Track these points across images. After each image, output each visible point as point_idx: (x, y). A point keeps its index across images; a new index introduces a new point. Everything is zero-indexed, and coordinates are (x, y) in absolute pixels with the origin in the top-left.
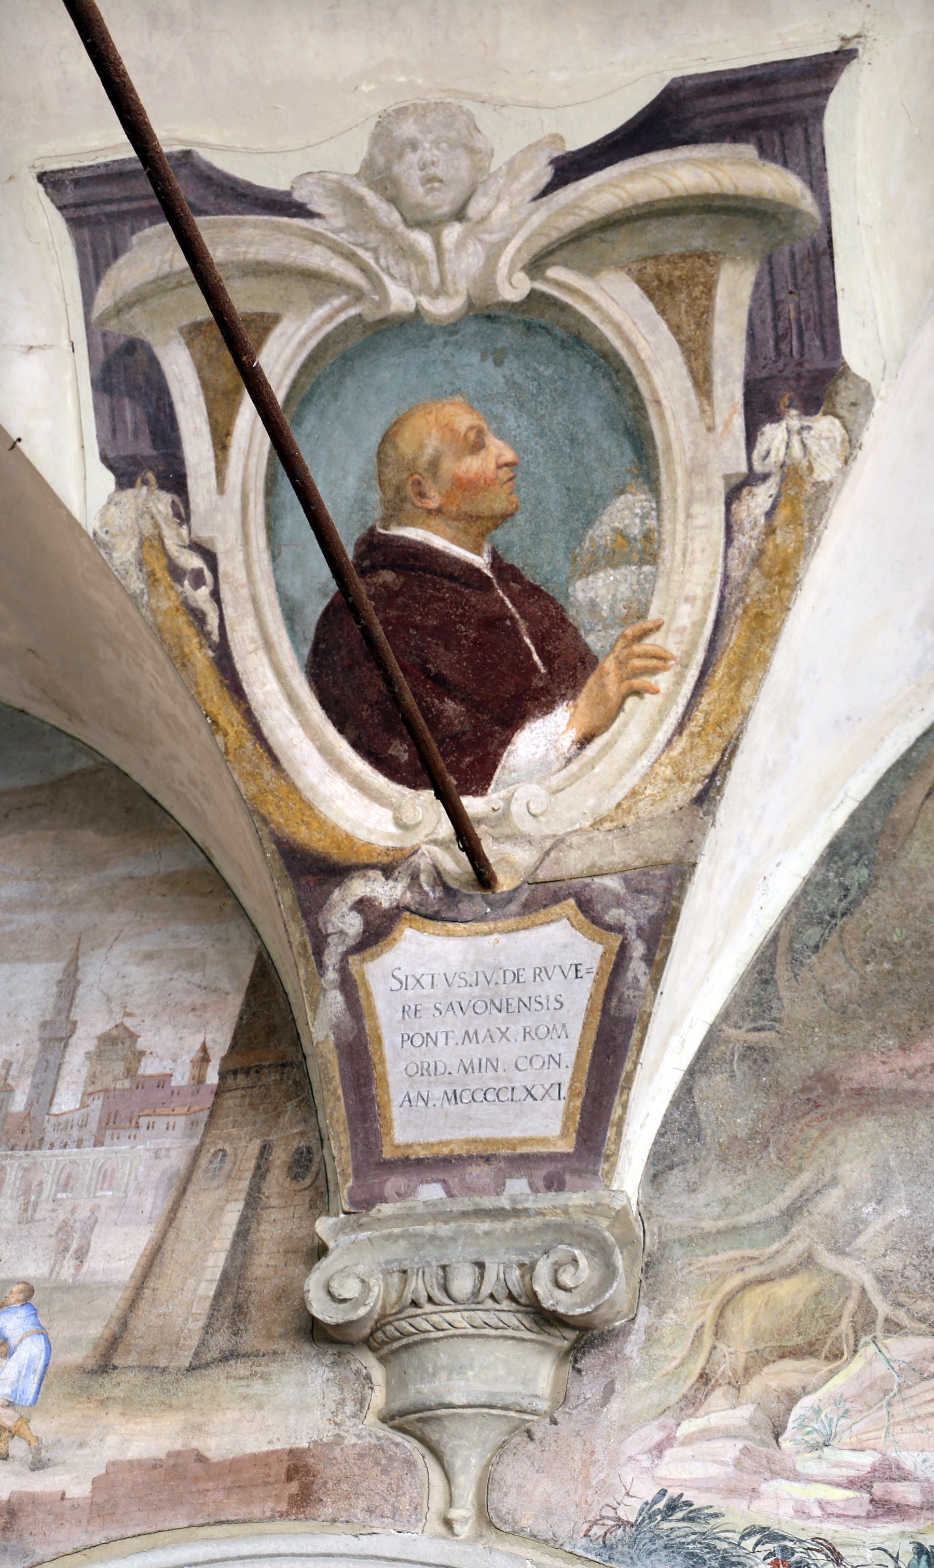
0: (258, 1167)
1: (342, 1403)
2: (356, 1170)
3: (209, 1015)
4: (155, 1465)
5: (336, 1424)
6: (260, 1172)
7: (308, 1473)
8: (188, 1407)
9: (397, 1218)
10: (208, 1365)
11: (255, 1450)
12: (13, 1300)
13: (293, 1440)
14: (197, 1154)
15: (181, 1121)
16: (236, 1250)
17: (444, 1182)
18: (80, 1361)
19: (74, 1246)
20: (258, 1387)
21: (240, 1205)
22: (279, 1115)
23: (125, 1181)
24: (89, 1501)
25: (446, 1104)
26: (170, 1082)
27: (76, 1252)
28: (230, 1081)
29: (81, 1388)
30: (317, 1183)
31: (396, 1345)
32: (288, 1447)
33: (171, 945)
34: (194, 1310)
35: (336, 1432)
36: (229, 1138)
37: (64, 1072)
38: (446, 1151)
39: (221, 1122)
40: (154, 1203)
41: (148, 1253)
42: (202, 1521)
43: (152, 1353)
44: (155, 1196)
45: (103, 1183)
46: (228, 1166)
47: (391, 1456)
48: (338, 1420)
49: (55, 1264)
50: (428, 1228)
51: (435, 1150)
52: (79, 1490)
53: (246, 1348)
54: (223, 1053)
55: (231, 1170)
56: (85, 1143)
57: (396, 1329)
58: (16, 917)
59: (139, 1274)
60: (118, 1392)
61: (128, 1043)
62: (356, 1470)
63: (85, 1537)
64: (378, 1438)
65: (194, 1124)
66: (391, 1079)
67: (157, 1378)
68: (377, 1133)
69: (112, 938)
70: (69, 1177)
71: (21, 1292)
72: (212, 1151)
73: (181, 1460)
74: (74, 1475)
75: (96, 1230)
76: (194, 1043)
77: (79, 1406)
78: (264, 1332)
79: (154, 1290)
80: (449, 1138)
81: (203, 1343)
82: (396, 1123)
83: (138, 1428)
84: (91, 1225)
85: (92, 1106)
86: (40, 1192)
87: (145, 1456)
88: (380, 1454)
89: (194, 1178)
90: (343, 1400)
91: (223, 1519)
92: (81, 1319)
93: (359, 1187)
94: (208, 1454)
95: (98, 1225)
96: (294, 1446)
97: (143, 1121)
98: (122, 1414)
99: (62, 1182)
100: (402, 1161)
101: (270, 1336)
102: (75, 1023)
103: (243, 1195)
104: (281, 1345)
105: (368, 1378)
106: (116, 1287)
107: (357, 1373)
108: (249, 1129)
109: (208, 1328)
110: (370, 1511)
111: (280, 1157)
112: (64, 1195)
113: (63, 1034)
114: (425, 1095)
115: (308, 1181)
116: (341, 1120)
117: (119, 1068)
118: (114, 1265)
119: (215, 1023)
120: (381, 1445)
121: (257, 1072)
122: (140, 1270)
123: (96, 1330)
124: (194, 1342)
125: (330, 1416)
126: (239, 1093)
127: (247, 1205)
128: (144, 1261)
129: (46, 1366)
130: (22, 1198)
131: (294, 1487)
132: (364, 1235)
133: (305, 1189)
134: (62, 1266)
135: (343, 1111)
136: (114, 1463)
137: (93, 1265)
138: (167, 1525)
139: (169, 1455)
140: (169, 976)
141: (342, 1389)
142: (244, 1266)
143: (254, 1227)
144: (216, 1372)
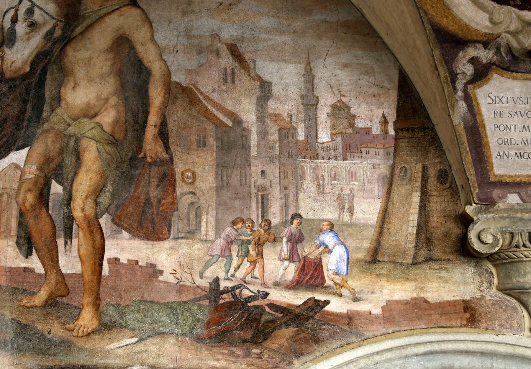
0: (423, 177)
1: (482, 282)
2: (478, 185)
3: (382, 100)
4: (407, 303)
5: (481, 291)
6: (425, 179)
7: (472, 310)
8: (415, 280)
9: (506, 210)
10: (420, 263)
11: (448, 299)
12: (325, 229)
13: (463, 296)
14: (393, 168)
15: (382, 151)
16: (421, 214)
17: (519, 193)
18: (363, 257)
19: (347, 207)
20: (444, 273)
21: (419, 194)
22: (427, 153)
23: (362, 178)
24: (382, 316)
25: (517, 159)
26: (372, 131)
27: (348, 209)
28: (400, 134)
29: (366, 269)
30: (452, 186)
31: (504, 261)
32: (462, 299)
33: (355, 61)
34: (408, 239)
35: (482, 294)
36: (406, 162)
37: (319, 122)
38: (518, 179)
39: (400, 153)
40: (378, 189)
41: (381, 212)
42: (432, 326)
43: (394, 256)
44: (378, 186)
45: (352, 178)
46: (409, 175)
47: (506, 305)
48: (481, 289)
49: (340, 214)
50: (519, 215)
51: (514, 179)
52: (377, 311)
53: (435, 257)
54: (394, 120)
55: (411, 177)
56: (339, 158)
57: (506, 255)
58: (272, 37)
59: (380, 221)
60: (383, 272)
61: (346, 111)
62: (492, 310)
63: (384, 330)
64: (500, 298)
65: (388, 153)
66: (491, 145)
67: (400, 267)
68: (486, 169)
69: (324, 54)
70: (335, 174)
71: (328, 225)
72: (400, 167)
73: (417, 301)
74: (373, 305)
75: (355, 200)
76: (379, 113)
77: (367, 276)
78: (442, 251)
79: (388, 229)
80: (520, 174)
81: (416, 254)
82: (495, 165)
83: (396, 287)
84: (352, 198)
85: (337, 140)
86: (324, 180)
87: (402, 299)
88: (502, 304)
89: (395, 179)
90: (482, 281)
91: (441, 326)
92: (358, 239)
93: (481, 193)
94: (429, 300)
95: (355, 197)
96: (465, 299)
97: (363, 150)
98: (387, 281)
99: (333, 176)
100: (499, 182)
101: (445, 253)
102: (317, 97)
103: (419, 189)
104: (451, 257)
105: (491, 273)
106: (371, 226)
107: (486, 270)
108: (415, 158)
109: (416, 247)
110: (501, 326)
111: (432, 172)
112: (335, 182)
113: (313, 103)
114: (507, 153)
115: (448, 185)
116: (470, 162)
117: (345, 123)
118: (367, 216)
119: (386, 104)
120: (502, 300)
121: (412, 131)
122: (379, 219)
123: (367, 245)
124: (412, 253)
125: (478, 287)
126: (406, 140)
127: (422, 193)
128: (380, 216)
129: (348, 258)
130: (316, 182)
131: (468, 315)
132: (490, 215)
133: (447, 189)
134: (343, 215)
135: (470, 158)
136: (389, 301)
137: (358, 216)
138: (417, 327)
139: (412, 299)
140: (358, 78)
141: (481, 277)
142: (427, 221)
143: (427, 204)
144: (424, 266)
